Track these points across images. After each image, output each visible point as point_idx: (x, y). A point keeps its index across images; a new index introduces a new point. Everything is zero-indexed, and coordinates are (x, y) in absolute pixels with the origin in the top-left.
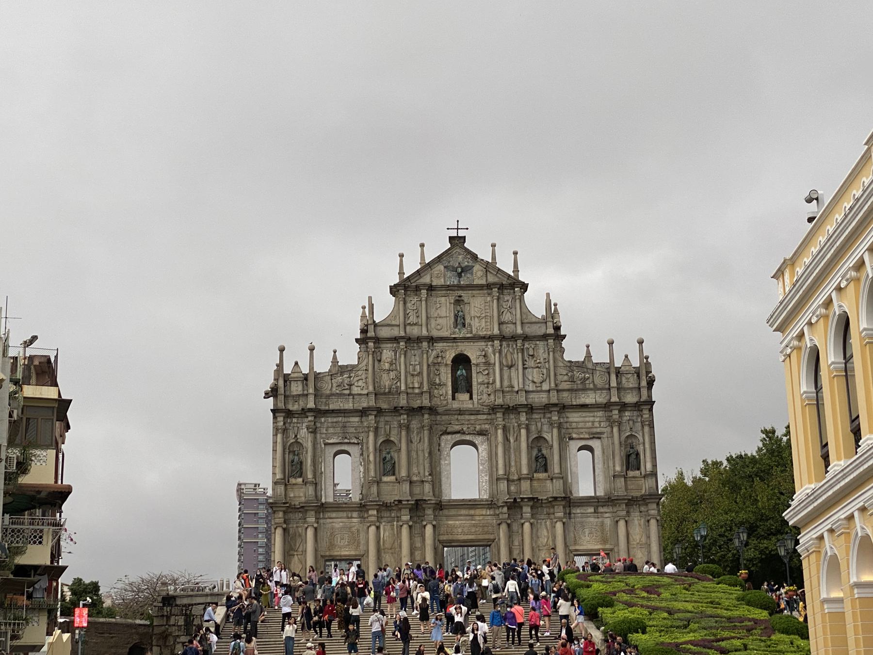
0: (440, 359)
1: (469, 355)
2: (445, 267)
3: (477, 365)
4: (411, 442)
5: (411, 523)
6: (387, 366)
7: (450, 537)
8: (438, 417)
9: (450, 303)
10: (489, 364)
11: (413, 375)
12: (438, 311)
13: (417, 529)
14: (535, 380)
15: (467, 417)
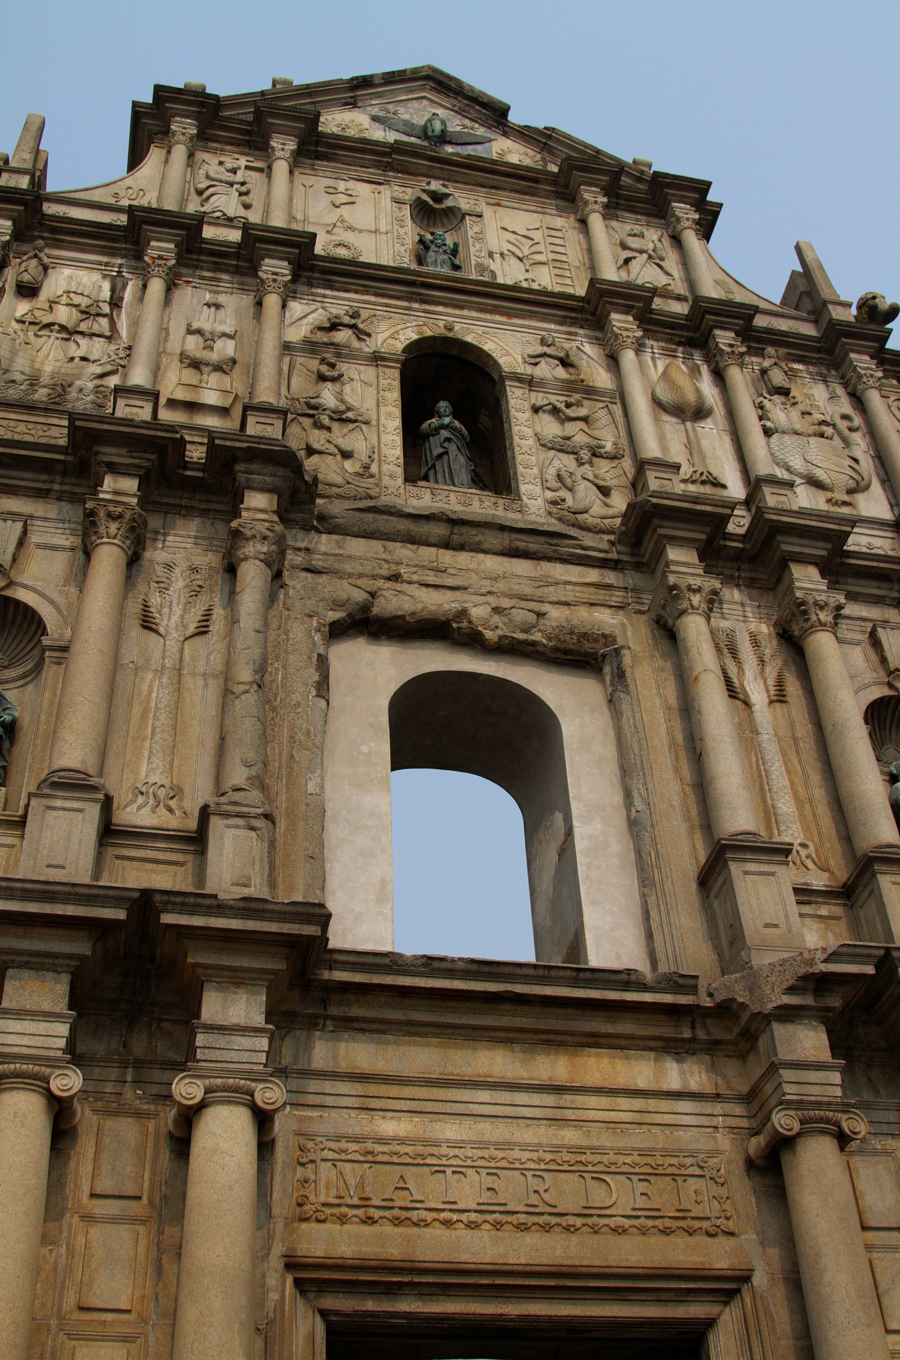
0: (343, 336)
1: (488, 347)
2: (375, 119)
3: (530, 383)
4: (148, 624)
5: (68, 1082)
6: (63, 315)
7: (387, 1243)
8: (325, 543)
9: (397, 201)
10: (590, 392)
11: (196, 365)
12: (345, 211)
13: (118, 1149)
14: (820, 475)
15: (491, 563)
